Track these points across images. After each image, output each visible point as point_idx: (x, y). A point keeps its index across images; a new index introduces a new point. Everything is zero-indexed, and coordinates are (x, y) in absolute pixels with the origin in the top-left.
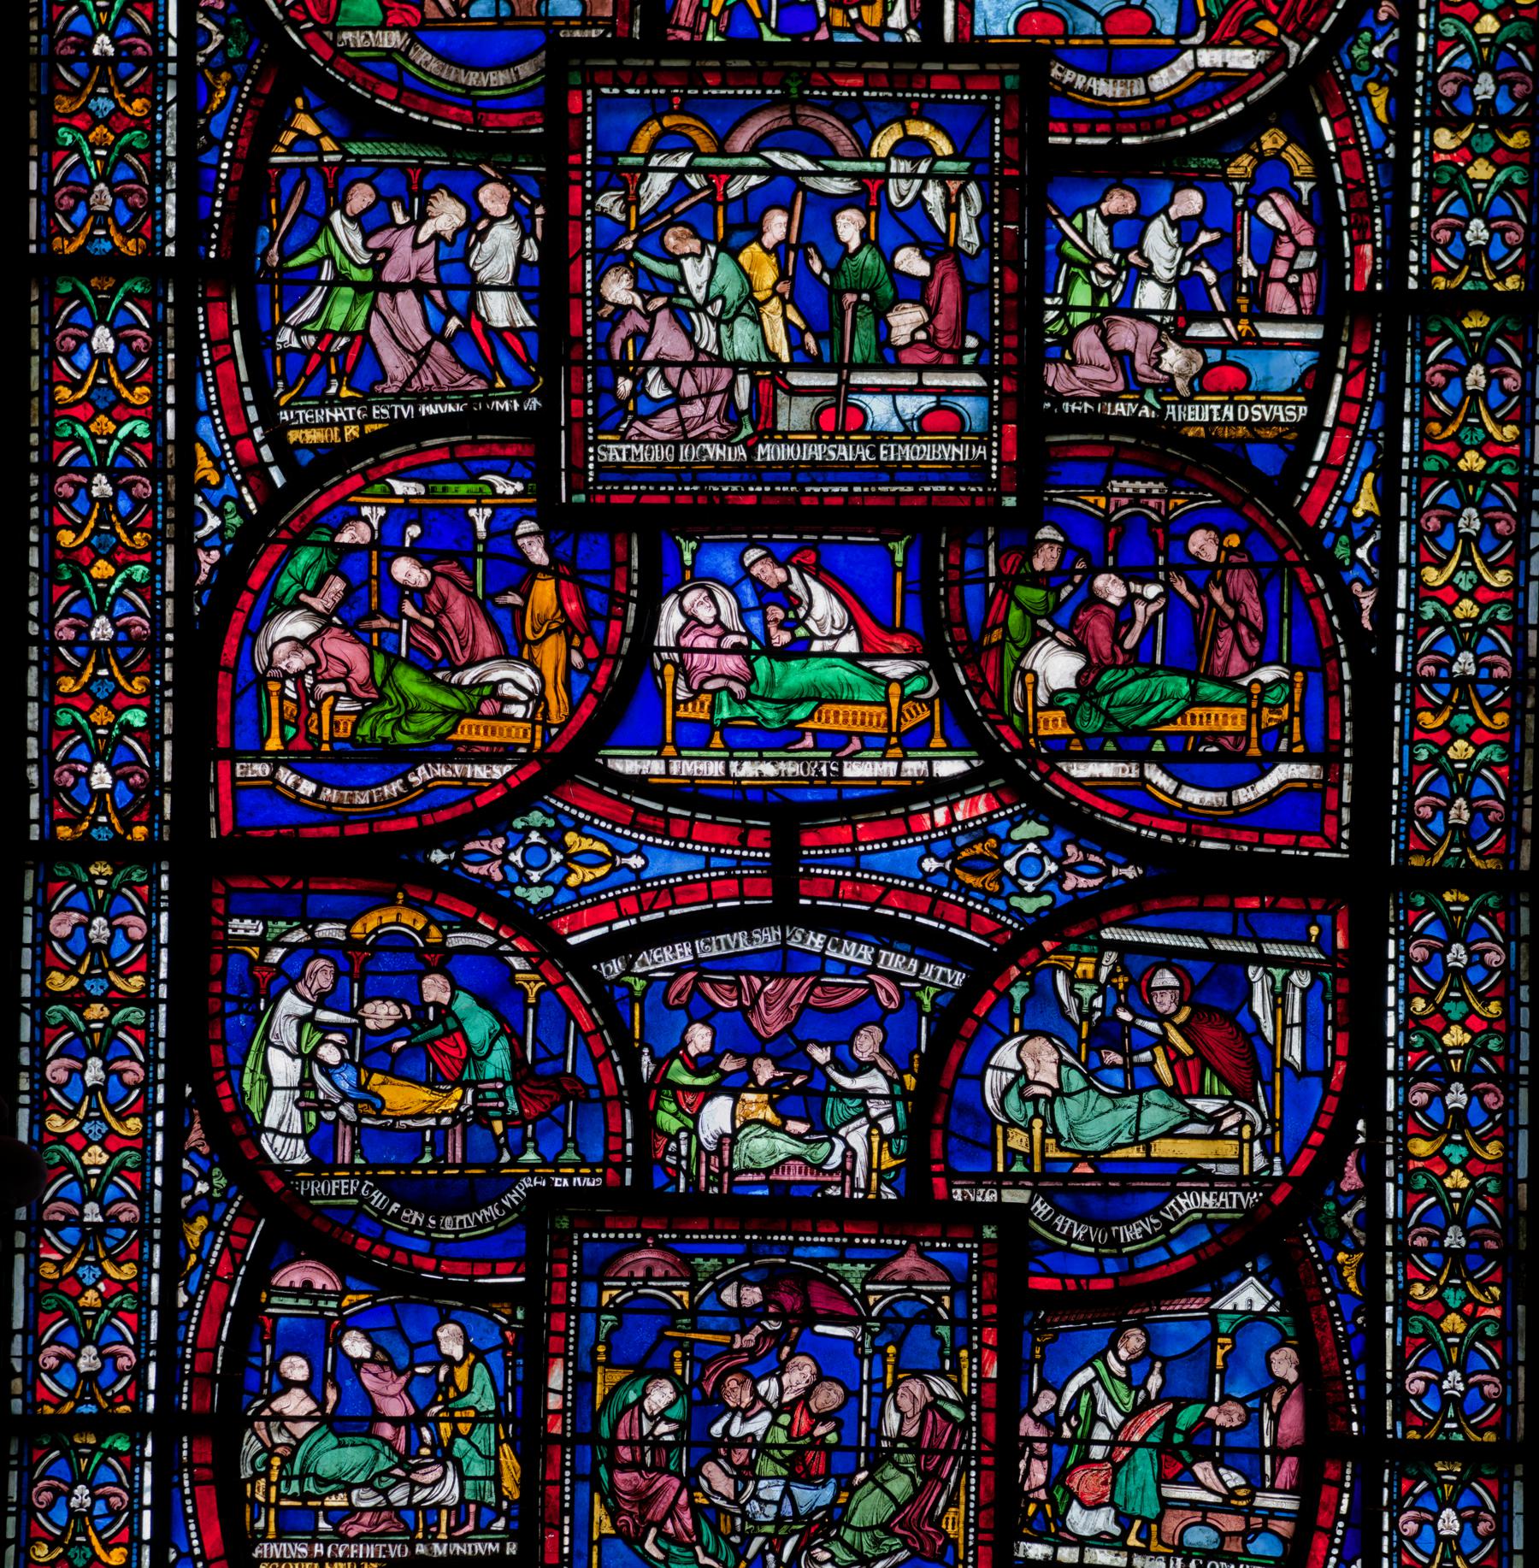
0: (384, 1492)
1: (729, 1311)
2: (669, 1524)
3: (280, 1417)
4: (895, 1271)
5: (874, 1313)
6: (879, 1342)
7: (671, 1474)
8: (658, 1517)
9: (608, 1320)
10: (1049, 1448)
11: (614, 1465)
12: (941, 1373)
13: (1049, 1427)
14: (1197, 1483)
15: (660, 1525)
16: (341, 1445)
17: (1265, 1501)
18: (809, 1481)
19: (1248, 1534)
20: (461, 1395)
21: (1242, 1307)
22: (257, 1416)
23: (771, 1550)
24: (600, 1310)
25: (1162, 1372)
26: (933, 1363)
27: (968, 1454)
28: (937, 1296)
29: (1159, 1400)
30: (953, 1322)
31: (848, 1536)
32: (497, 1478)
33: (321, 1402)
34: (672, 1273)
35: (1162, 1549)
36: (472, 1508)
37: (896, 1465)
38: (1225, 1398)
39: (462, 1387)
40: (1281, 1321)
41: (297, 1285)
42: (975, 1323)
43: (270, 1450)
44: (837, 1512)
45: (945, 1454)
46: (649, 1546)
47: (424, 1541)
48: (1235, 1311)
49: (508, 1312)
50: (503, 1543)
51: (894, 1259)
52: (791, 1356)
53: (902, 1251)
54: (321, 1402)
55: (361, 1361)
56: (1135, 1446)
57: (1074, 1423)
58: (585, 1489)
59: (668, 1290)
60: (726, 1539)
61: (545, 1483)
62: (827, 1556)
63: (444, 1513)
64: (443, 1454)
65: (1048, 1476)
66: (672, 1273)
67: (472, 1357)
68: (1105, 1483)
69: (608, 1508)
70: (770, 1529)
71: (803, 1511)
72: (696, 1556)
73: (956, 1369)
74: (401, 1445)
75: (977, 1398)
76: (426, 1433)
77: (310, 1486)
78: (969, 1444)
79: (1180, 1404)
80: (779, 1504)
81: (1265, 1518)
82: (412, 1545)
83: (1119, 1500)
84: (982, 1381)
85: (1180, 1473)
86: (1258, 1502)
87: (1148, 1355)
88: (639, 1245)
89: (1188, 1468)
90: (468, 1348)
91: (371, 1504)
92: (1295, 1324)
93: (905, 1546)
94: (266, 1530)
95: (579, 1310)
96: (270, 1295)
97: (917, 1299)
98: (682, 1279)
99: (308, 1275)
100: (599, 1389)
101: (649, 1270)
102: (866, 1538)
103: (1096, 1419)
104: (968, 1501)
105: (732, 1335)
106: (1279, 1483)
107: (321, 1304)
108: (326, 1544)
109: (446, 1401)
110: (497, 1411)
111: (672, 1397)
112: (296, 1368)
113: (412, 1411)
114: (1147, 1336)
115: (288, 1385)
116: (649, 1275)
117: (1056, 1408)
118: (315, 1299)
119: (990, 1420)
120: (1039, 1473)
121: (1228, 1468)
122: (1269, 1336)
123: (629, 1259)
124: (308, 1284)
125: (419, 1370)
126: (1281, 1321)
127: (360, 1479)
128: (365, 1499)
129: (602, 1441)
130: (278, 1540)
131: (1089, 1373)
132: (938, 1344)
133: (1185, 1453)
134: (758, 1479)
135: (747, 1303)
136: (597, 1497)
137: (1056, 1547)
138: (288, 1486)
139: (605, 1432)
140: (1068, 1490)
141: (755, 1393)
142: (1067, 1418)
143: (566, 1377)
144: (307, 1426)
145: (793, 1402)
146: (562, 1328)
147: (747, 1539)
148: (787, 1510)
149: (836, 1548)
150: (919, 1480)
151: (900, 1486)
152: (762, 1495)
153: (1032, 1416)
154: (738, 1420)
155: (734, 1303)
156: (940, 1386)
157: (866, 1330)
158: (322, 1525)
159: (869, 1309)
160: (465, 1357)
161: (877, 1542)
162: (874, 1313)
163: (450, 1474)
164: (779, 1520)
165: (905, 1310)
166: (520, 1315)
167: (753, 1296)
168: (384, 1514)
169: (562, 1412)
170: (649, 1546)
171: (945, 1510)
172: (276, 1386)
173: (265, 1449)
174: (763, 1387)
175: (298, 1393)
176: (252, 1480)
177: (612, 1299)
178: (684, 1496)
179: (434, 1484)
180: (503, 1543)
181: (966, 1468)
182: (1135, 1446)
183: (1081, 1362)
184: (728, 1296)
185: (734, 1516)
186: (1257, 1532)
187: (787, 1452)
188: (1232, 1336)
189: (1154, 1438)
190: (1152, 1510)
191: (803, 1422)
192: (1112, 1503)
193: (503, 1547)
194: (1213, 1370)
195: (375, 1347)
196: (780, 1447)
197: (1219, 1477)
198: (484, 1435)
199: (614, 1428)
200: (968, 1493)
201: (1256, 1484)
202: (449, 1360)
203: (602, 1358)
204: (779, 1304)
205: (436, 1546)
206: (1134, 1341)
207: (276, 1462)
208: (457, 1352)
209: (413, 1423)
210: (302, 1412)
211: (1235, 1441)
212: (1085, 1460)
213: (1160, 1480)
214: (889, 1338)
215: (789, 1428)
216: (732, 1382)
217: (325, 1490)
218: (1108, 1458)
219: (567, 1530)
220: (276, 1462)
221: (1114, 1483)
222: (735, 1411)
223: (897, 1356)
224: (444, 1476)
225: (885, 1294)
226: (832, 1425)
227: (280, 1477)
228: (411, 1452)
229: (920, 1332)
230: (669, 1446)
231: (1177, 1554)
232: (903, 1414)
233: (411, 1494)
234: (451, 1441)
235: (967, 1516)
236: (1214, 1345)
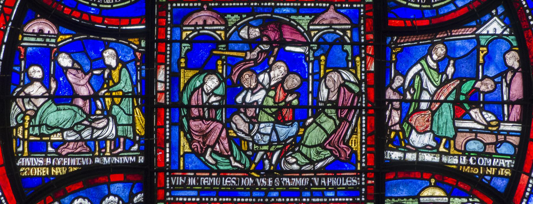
0: (79, 133)
1: (244, 41)
2: (217, 146)
3: (29, 96)
4: (324, 19)
5: (314, 40)
6: (317, 54)
7: (218, 121)
8: (212, 143)
9: (186, 47)
10: (401, 104)
11: (189, 117)
12: (347, 69)
13: (400, 94)
14: (472, 119)
15: (213, 147)
16: (58, 110)
17: (505, 127)
18: (284, 122)
19: (497, 144)
20: (115, 84)
21: (491, 32)
22: (18, 96)
23: (267, 158)
24: (181, 41)
25: (454, 65)
26: (343, 64)
27: (361, 108)
28: (344, 31)
29: (453, 78)
30: (352, 44)
31: (304, 150)
32: (133, 125)
33: (48, 88)
34: (216, 22)
35: (456, 153)
36: (122, 140)
37: (327, 115)
38: (485, 77)
39: (116, 80)
40: (511, 38)
41: (36, 31)
42: (363, 44)
43: (24, 113)
44: (298, 139)
45: (350, 108)
46: (207, 157)
47: (99, 156)
48: (488, 34)
49: (137, 43)
50: (137, 157)
51: (323, 13)
52: (274, 62)
53: (326, 9)
54: (48, 88)
55: (67, 68)
56: (442, 102)
57: (412, 92)
58: (176, 129)
59: (214, 31)
60: (245, 152)
61: (158, 127)
62: (294, 160)
63: (108, 142)
64: (107, 114)
65: (401, 117)
66: (216, 22)
67: (120, 65)
68: (428, 121)
69: (187, 139)
70: (266, 148)
71: (282, 138)
72: (230, 162)
73: (354, 67)
74: (87, 109)
75: (365, 80)
76: (99, 103)
77: (44, 130)
78: (361, 103)
79: (463, 80)
80: (270, 135)
81: (505, 136)
82: (93, 158)
83: (435, 129)
84: (367, 73)
85: (465, 115)
86: (502, 128)
87: (447, 57)
88: (200, 9)
89: (468, 112)
90: (118, 61)
91: (73, 138)
92: (517, 40)
93: (332, 154)
94: (22, 152)
95: (171, 42)
96: (23, 36)
97: (334, 32)
98: (221, 25)
99: (41, 26)
100: (183, 81)
101: (205, 21)
102: (313, 151)
103: (422, 89)
104: (362, 132)
105: (246, 52)
106: (511, 119)
107: (48, 40)
108: (52, 158)
109: (109, 87)
110: (133, 92)
111: (217, 83)
112: (36, 72)
113: (92, 92)
114: (446, 48)
115: (32, 81)
116: (205, 24)
117: (403, 85)
118: (45, 38)
119: (372, 91)
120: (396, 117)
121: (487, 111)
122: (504, 46)
123: (195, 15)
124: (41, 31)
125: (96, 72)
126: (511, 38)
127: (68, 126)
128: (71, 136)
129: (184, 106)
130: (29, 156)
131: (418, 67)
132: (345, 54)
133: (466, 105)
134: (260, 123)
135: (252, 37)
136: (182, 134)
137: (405, 153)
138: (33, 130)
139: (185, 102)
140: (410, 125)
141: (257, 81)
142: (409, 89)
143: (166, 75)
144: (42, 101)
145: (276, 85)
146: (164, 51)
147: (255, 153)
148: (274, 138)
149: (298, 156)
150: (338, 122)
151: (329, 125)
152: (262, 131)
153: (392, 88)
154: (249, 94)
155: (247, 37)
156: (346, 75)
157: (311, 48)
158: (50, 149)
159: (311, 38)
160: (117, 65)
161: (318, 153)
162: (314, 40)
163: (111, 123)
164: (270, 144)
165: (329, 38)
166: (143, 44)
167: (255, 33)
168: (80, 143)
169: (164, 92)
170: (207, 157)
171: (351, 136)
172: (27, 81)
173: (22, 112)
174: (261, 77)
175: (38, 84)
176: (16, 127)
177: (187, 36)
178: (224, 132)
179: (103, 128)
180: (137, 157)
181: (360, 115)
182: (442, 102)
183: (414, 61)
184: (243, 33)
185: (248, 142)
186: (502, 143)
187: (274, 110)
188: (487, 46)
189: (451, 98)
190: (451, 133)
191: (281, 94)
192: (431, 131)
193: (137, 159)
194: (478, 63)
195: (74, 61)
196: (270, 107)
197: (483, 116)
198: (127, 104)
199: (189, 100)
200: (361, 128)
201: (500, 119)
202: (110, 67)
203: (183, 65)
204: (268, 37)
205: (105, 159)
206: (440, 50)
207: (27, 118)
208: (113, 63)
209: (92, 98)
210: (39, 93)
211: (489, 97)
212: (418, 110)
213: (455, 118)
214: (322, 52)
215: (274, 98)
216: (246, 75)
217: (51, 132)
218: (429, 109)
219: (168, 150)
220: (27, 118)
221: (432, 120)
222: (248, 89)
223: (326, 61)
224: (108, 124)
225: (319, 30)
226: (295, 95)
227: (30, 126)
228: (92, 112)
229: (337, 49)
230: (216, 108)
231: (464, 155)
232: (329, 89)
233: (92, 133)
234: (111, 108)
235: (361, 139)
236: (478, 51)
